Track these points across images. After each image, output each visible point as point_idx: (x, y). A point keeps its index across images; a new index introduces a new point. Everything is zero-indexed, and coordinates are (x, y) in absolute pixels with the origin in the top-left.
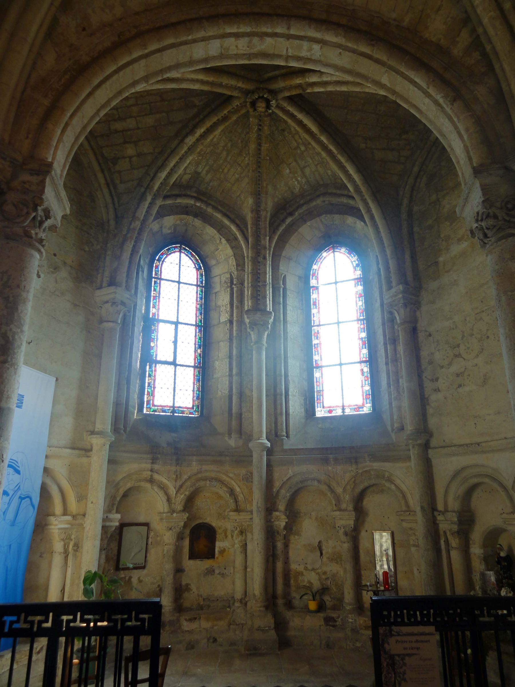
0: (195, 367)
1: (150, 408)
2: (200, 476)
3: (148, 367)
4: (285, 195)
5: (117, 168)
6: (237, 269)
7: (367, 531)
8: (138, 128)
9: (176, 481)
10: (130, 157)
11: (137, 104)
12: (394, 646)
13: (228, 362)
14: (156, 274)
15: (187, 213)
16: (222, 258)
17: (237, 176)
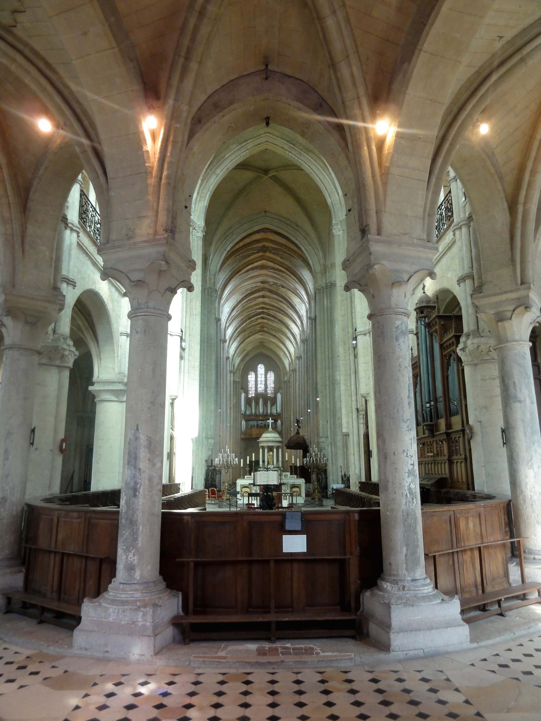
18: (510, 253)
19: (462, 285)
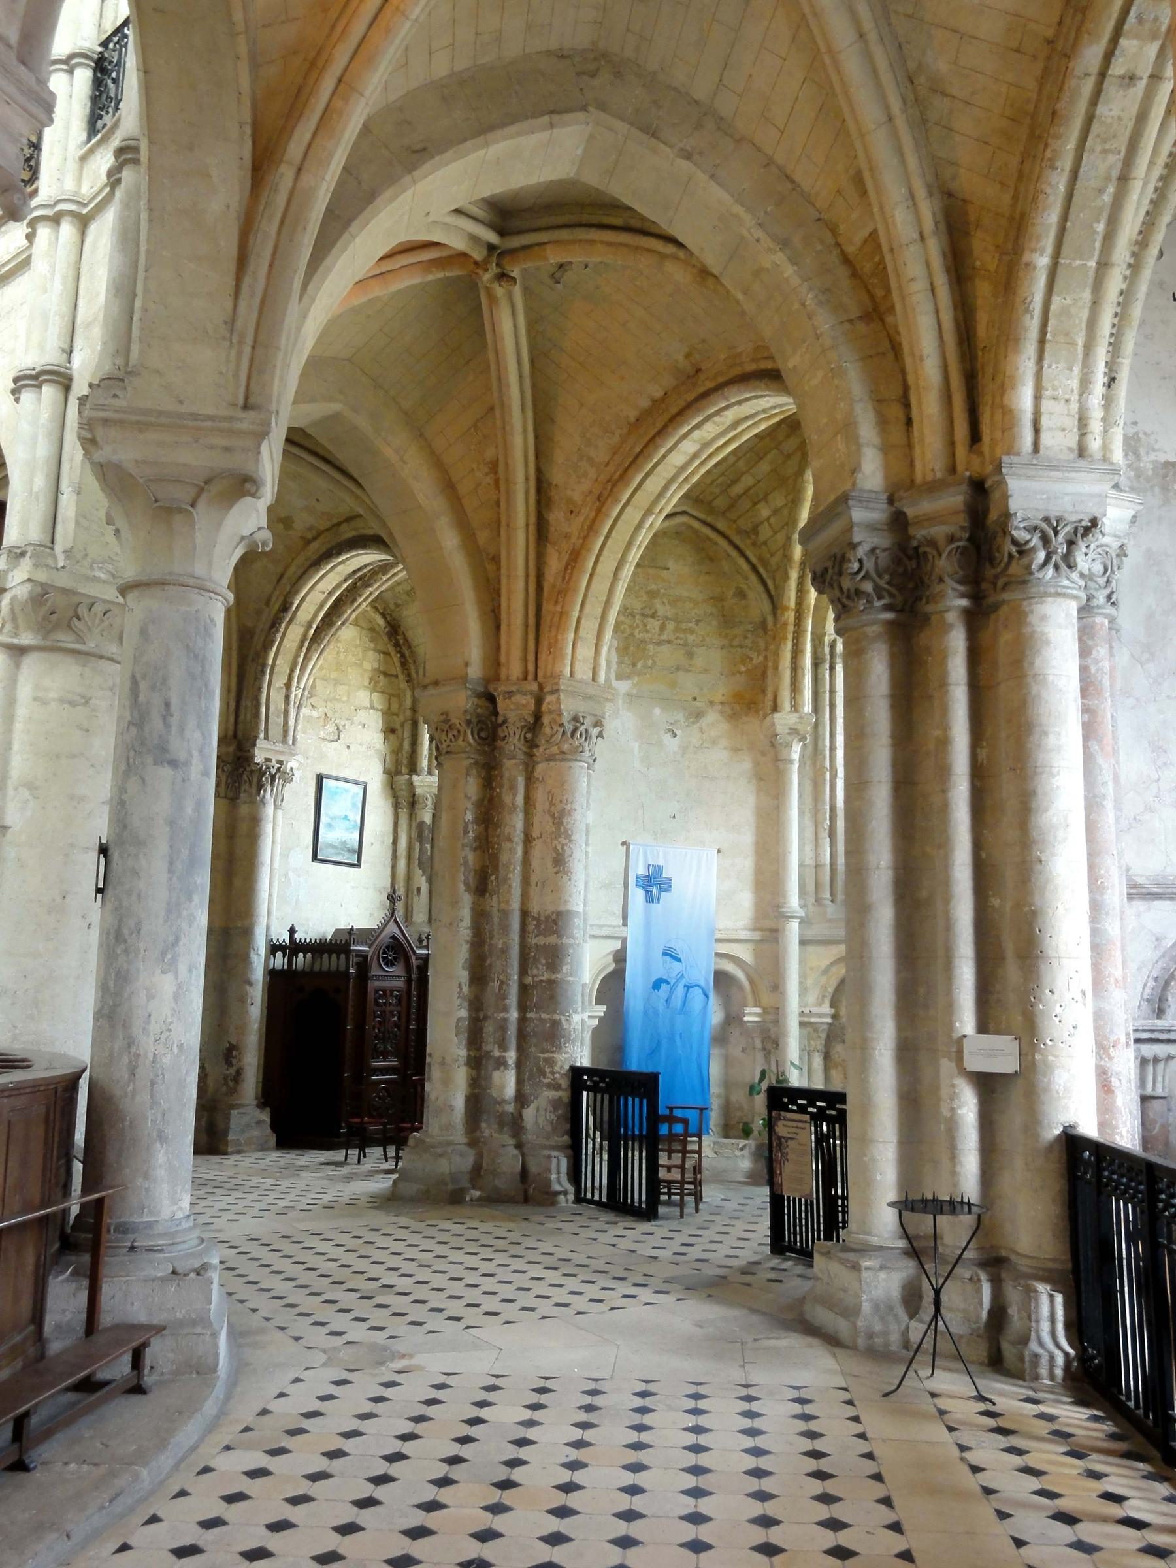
5: (762, 538)
8: (759, 481)
10: (768, 519)
11: (739, 459)
12: (781, 1129)
18: (229, 304)
19: (27, 396)
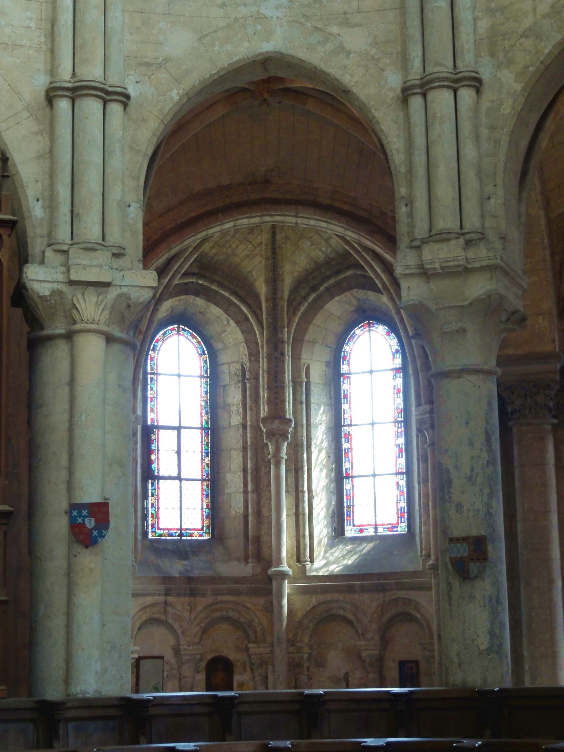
0: (202, 480)
1: (155, 532)
2: (214, 607)
3: (150, 485)
4: (307, 266)
6: (250, 360)
7: (394, 661)
9: (190, 613)
13: (242, 476)
14: (152, 369)
15: (187, 293)
16: (230, 343)
17: (247, 252)
